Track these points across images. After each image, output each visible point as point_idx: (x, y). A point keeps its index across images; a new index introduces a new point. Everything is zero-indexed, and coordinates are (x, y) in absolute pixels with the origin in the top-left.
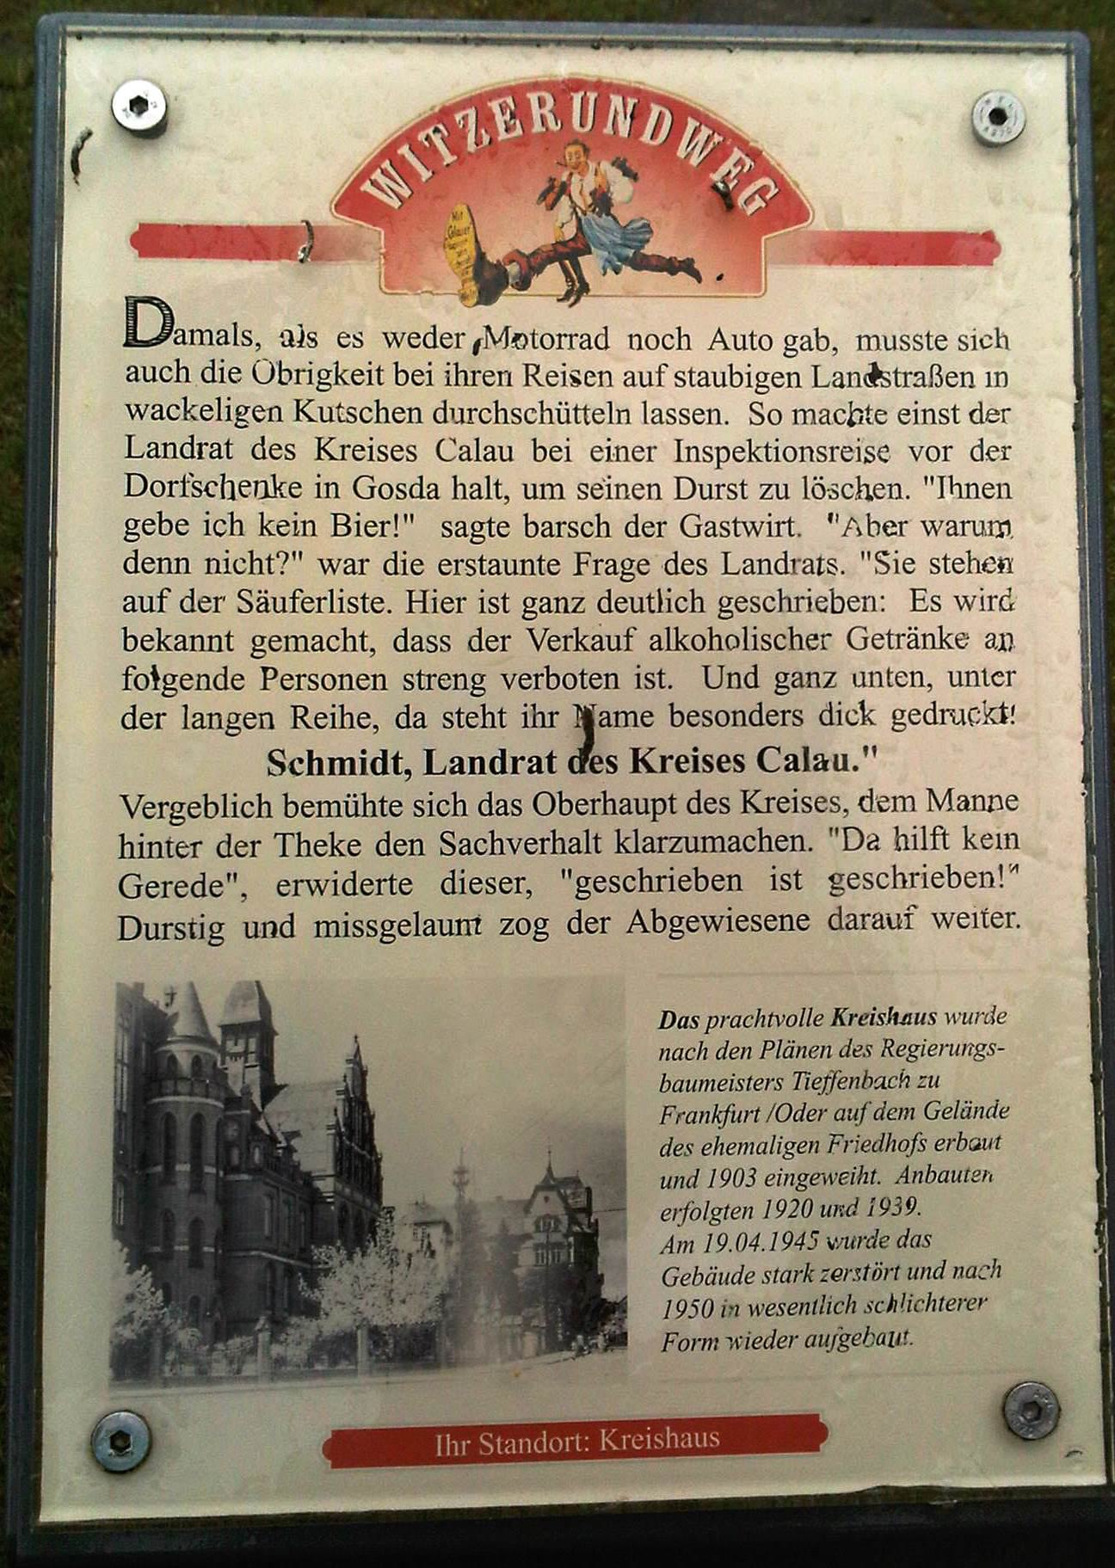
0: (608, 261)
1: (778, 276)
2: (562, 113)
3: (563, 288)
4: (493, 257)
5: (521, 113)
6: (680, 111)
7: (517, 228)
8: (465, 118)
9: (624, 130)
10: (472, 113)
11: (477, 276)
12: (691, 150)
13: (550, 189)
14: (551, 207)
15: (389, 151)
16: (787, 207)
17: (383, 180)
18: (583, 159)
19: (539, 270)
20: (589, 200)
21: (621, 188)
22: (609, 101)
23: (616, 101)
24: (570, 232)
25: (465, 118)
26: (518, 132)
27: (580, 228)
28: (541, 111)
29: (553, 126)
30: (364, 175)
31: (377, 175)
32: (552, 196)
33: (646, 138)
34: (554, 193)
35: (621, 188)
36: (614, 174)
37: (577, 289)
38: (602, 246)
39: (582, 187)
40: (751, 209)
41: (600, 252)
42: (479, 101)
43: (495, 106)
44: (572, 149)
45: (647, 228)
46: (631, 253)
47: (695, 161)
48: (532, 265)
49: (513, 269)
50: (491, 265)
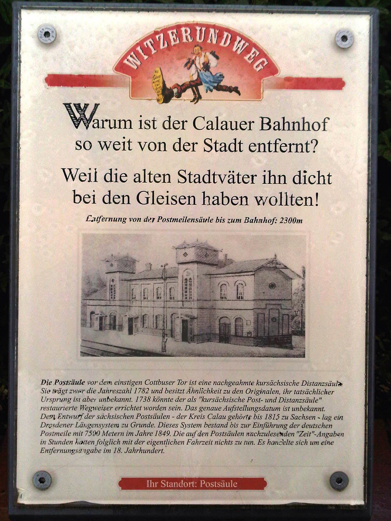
0: (208, 87)
1: (267, 93)
2: (193, 34)
3: (192, 97)
4: (169, 85)
5: (179, 35)
6: (234, 35)
7: (178, 76)
8: (159, 38)
9: (214, 42)
10: (162, 35)
11: (163, 93)
12: (238, 47)
13: (189, 62)
14: (189, 69)
15: (133, 49)
16: (271, 69)
17: (131, 59)
18: (200, 51)
19: (184, 91)
20: (202, 66)
21: (213, 62)
22: (209, 31)
23: (212, 31)
24: (195, 77)
25: (159, 38)
26: (178, 42)
27: (198, 76)
28: (185, 34)
29: (190, 40)
30: (125, 57)
31: (129, 57)
32: (189, 65)
33: (222, 44)
34: (190, 64)
35: (213, 62)
36: (211, 57)
37: (197, 98)
38: (206, 82)
39: (200, 61)
40: (258, 69)
41: (206, 84)
42: (165, 31)
43: (170, 32)
44: (197, 48)
45: (222, 76)
46: (216, 85)
47: (239, 52)
48: (182, 89)
49: (175, 91)
50: (168, 89)
